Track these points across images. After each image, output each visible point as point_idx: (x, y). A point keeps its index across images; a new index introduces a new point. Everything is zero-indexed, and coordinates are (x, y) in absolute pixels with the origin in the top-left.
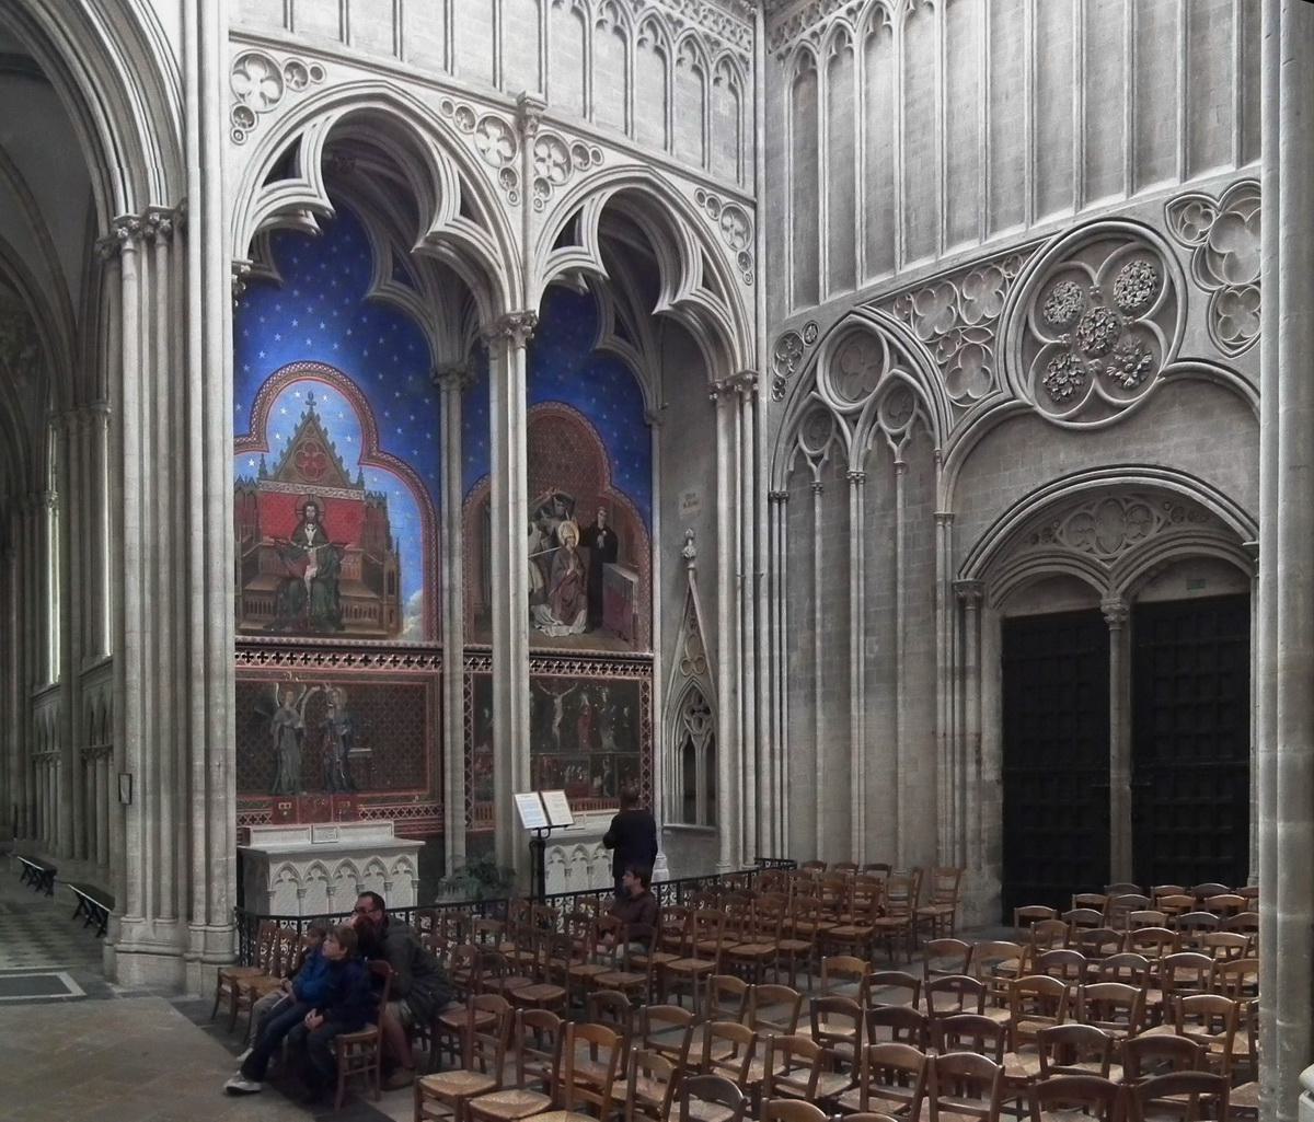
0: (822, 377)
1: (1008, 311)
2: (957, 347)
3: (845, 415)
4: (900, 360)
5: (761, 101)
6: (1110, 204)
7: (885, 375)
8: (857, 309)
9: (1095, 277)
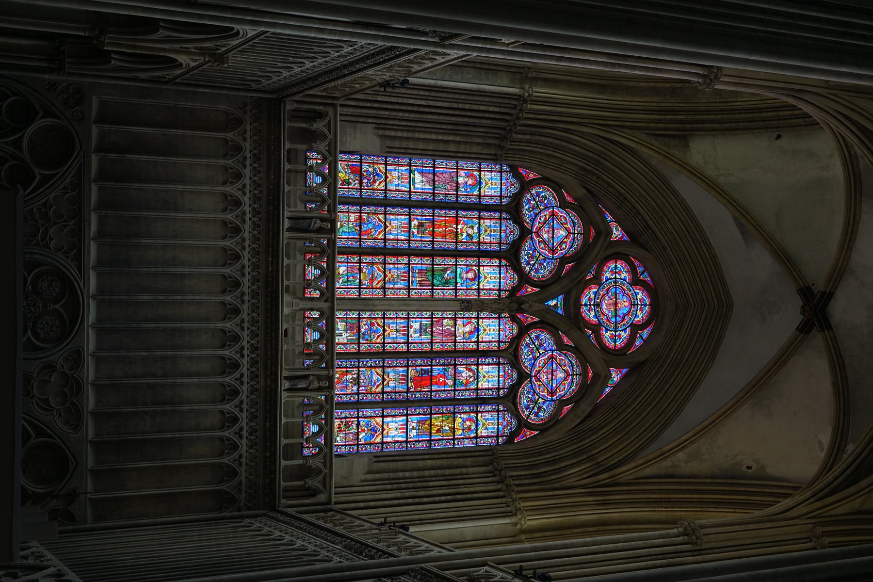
0: (49, 121)
1: (51, 256)
2: (40, 222)
3: (22, 137)
4: (45, 179)
5: (225, 92)
6: (92, 313)
7: (36, 170)
8: (82, 153)
9: (57, 306)
